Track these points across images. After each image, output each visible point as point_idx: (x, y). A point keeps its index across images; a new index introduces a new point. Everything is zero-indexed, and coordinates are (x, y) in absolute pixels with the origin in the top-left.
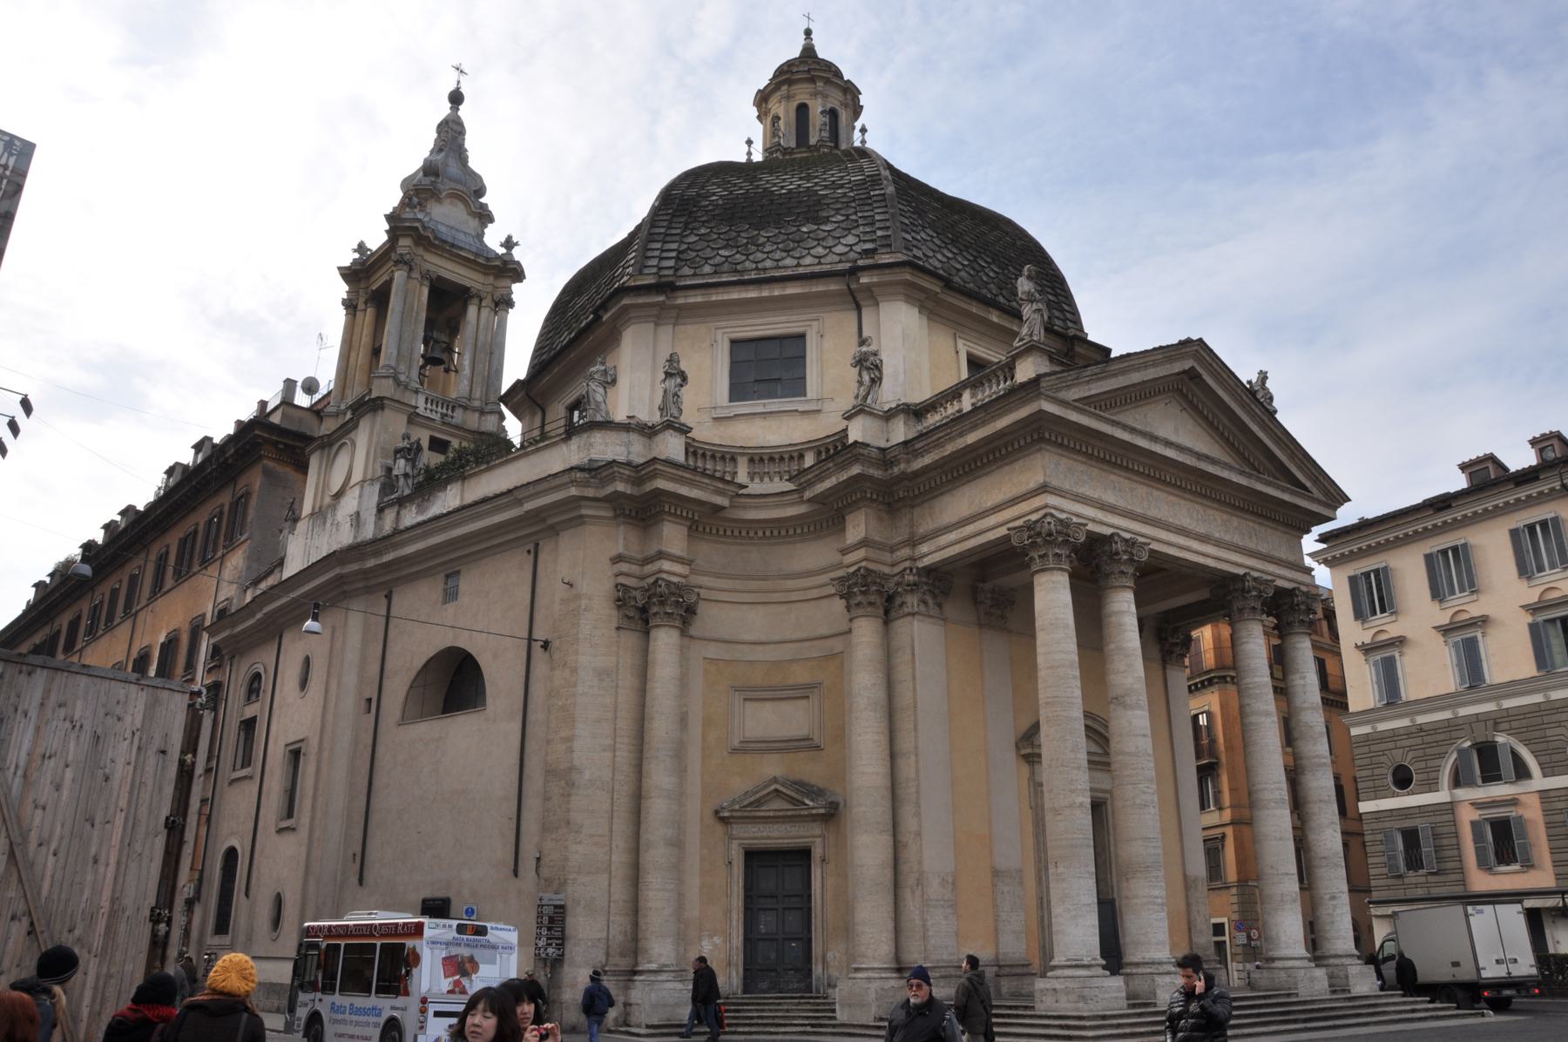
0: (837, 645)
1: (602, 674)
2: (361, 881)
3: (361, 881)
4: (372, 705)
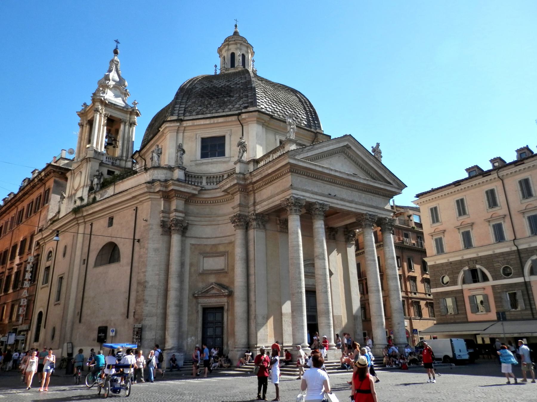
0: (232, 238)
1: (156, 250)
2: (80, 321)
3: (80, 321)
4: (85, 262)
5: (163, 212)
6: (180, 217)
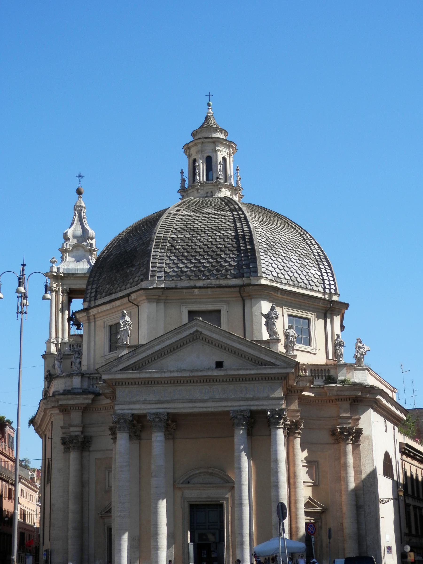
5: (62, 428)
6: (76, 431)
